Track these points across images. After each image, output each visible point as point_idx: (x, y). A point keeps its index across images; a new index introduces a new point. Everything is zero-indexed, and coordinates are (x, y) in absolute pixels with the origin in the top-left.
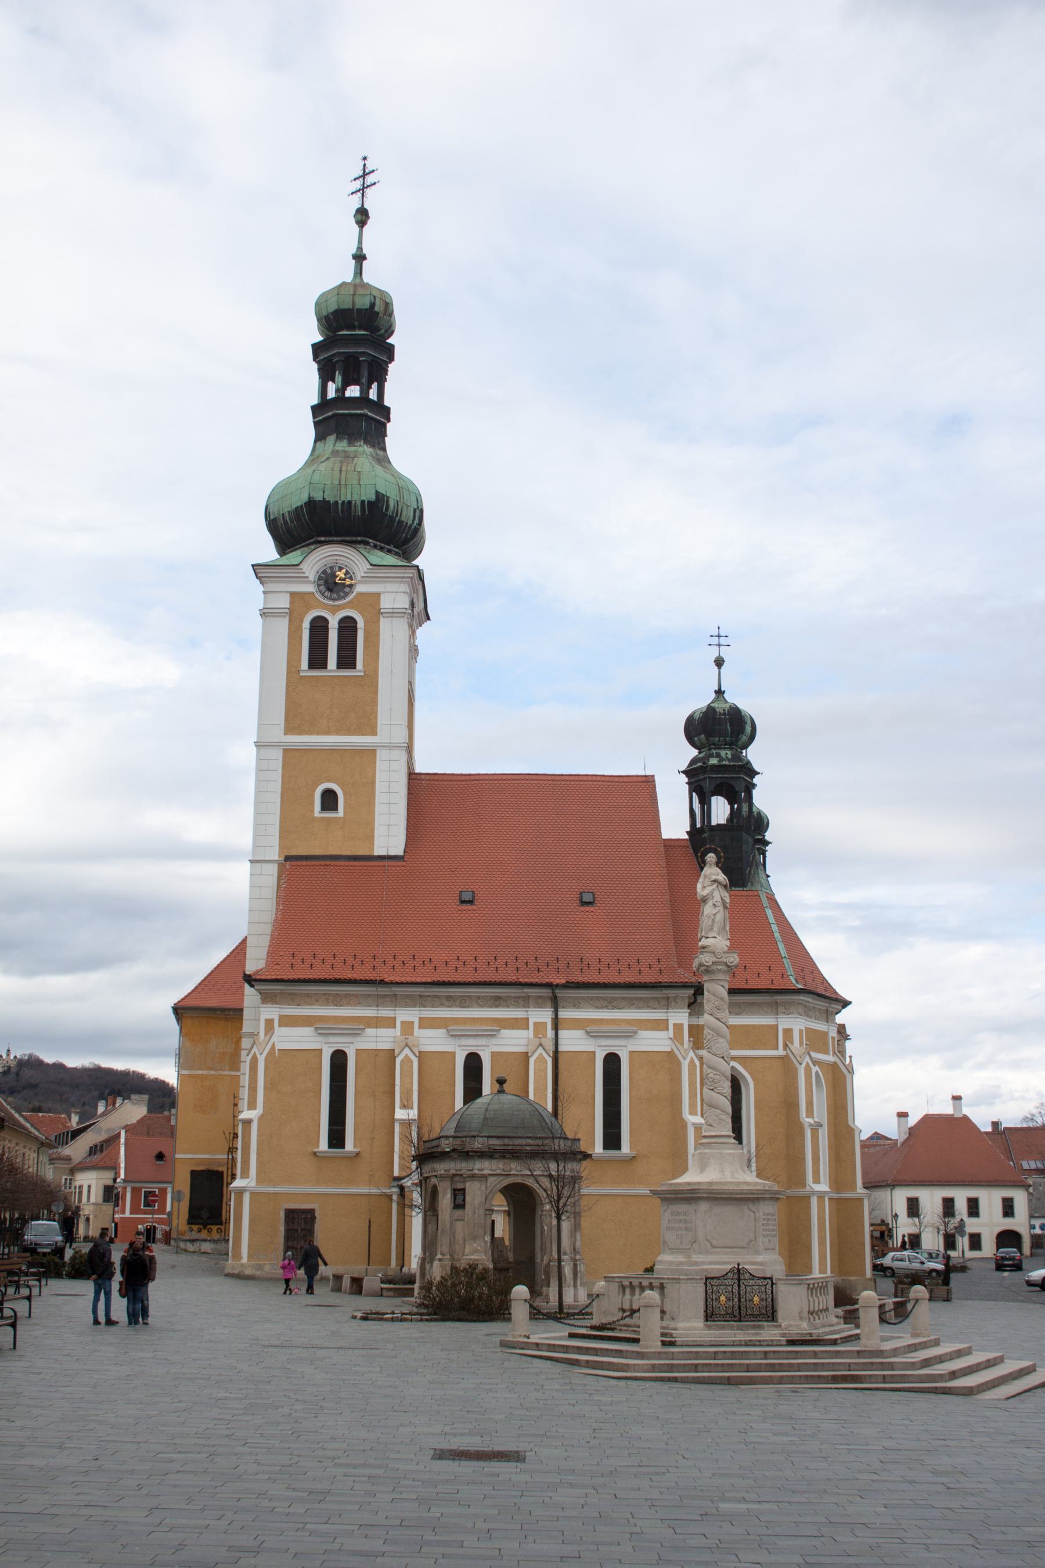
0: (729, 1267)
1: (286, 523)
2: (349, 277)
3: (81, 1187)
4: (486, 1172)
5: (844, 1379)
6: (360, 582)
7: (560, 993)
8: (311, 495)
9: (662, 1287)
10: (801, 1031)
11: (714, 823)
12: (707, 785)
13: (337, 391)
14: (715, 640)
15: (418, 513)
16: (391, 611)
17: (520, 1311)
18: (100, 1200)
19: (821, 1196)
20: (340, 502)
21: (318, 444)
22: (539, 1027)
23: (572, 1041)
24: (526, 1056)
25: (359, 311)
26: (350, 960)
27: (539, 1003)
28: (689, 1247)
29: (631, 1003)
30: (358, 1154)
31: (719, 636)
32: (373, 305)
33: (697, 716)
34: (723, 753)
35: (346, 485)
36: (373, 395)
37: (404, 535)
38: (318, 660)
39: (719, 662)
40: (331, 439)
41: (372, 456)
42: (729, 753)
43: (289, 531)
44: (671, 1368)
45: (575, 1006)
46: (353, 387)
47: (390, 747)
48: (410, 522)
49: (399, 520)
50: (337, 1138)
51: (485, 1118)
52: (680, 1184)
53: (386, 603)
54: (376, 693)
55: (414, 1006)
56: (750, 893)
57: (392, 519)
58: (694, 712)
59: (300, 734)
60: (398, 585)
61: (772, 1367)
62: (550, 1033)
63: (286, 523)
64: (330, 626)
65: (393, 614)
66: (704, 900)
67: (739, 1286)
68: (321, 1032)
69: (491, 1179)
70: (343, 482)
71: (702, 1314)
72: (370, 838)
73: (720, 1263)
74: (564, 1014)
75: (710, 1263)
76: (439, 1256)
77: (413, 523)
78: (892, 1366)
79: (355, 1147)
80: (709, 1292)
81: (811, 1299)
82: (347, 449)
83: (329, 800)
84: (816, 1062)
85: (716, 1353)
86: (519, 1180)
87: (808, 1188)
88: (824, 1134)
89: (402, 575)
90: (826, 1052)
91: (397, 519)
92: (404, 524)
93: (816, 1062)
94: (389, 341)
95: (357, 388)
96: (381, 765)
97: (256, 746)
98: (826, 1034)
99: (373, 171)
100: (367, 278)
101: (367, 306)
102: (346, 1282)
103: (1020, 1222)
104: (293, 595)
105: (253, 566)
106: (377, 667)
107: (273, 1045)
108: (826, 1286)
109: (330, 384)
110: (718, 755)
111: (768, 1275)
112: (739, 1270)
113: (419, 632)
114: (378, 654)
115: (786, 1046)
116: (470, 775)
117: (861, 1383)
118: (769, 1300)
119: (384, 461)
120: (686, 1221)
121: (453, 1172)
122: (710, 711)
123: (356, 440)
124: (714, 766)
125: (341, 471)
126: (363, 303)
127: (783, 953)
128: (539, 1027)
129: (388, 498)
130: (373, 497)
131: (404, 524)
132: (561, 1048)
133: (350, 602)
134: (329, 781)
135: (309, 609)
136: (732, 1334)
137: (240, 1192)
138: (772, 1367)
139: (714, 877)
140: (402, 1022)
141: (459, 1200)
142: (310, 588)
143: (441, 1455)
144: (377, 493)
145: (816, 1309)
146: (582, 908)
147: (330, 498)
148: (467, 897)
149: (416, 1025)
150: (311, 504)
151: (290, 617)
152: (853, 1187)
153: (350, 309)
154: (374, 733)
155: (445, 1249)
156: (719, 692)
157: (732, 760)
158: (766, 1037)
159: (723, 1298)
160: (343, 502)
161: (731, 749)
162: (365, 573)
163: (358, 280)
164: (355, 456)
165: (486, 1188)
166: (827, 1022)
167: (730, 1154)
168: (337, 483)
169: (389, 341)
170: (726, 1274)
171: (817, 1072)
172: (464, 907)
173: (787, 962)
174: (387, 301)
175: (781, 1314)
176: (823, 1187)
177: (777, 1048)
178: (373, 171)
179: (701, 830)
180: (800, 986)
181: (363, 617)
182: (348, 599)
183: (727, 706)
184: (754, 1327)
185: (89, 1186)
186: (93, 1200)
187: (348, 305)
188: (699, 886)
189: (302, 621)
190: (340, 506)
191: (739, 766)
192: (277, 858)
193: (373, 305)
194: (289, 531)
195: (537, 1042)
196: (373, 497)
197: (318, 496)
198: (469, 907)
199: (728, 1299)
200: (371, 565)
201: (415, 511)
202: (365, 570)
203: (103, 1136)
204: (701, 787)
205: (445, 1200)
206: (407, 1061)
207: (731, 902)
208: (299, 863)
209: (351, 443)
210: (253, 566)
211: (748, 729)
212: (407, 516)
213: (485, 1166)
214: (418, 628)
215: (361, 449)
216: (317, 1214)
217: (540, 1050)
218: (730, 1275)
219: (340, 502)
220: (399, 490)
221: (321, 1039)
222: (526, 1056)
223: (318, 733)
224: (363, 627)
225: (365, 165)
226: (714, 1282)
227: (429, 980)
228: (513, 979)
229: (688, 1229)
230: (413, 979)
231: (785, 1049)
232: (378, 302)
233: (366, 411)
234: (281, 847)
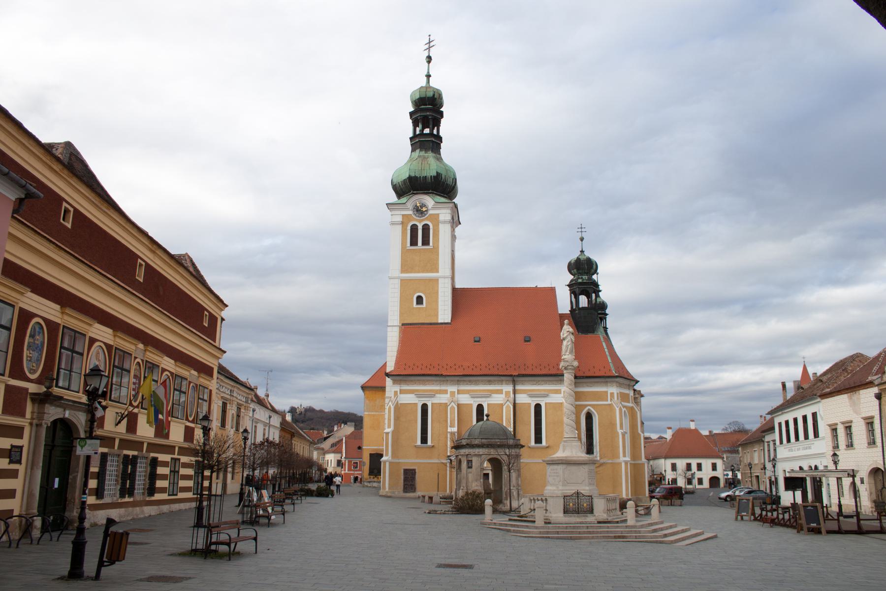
0: (574, 491)
1: (400, 186)
2: (424, 84)
3: (328, 460)
4: (481, 453)
5: (619, 537)
6: (431, 209)
7: (516, 379)
9: (546, 500)
10: (618, 393)
11: (581, 306)
12: (577, 291)
13: (420, 131)
14: (580, 230)
17: (488, 510)
18: (336, 466)
19: (626, 463)
21: (413, 153)
22: (507, 393)
23: (522, 399)
25: (428, 98)
26: (429, 366)
28: (557, 483)
29: (546, 382)
30: (433, 446)
31: (581, 228)
32: (434, 95)
33: (573, 262)
34: (584, 277)
35: (424, 169)
36: (435, 132)
38: (414, 242)
39: (582, 239)
40: (418, 151)
41: (435, 157)
42: (586, 277)
43: (401, 189)
44: (548, 533)
45: (522, 384)
46: (426, 129)
47: (444, 277)
48: (451, 184)
50: (424, 440)
51: (480, 431)
52: (554, 457)
53: (442, 218)
55: (455, 385)
56: (596, 336)
58: (572, 260)
60: (446, 210)
61: (590, 533)
62: (512, 395)
63: (400, 186)
64: (419, 228)
65: (445, 222)
66: (564, 339)
67: (578, 499)
68: (419, 396)
69: (483, 456)
70: (423, 168)
71: (562, 511)
72: (437, 315)
73: (570, 490)
74: (518, 387)
75: (566, 490)
76: (462, 488)
78: (640, 532)
79: (432, 443)
80: (566, 501)
81: (609, 505)
83: (420, 300)
84: (624, 407)
85: (566, 527)
86: (495, 456)
87: (621, 459)
88: (628, 437)
90: (629, 402)
93: (624, 407)
94: (441, 110)
95: (428, 129)
98: (628, 395)
100: (431, 84)
101: (432, 95)
102: (427, 498)
103: (719, 473)
104: (403, 215)
107: (398, 402)
108: (616, 499)
109: (417, 128)
110: (582, 278)
111: (590, 495)
112: (578, 493)
113: (457, 229)
115: (611, 400)
116: (478, 288)
117: (626, 539)
118: (591, 505)
119: (439, 159)
120: (557, 473)
121: (467, 453)
122: (578, 259)
123: (428, 150)
124: (580, 283)
125: (422, 164)
126: (430, 94)
127: (610, 361)
129: (442, 174)
130: (435, 174)
132: (517, 402)
133: (427, 218)
134: (419, 292)
135: (410, 221)
136: (574, 519)
137: (385, 462)
138: (590, 533)
139: (568, 330)
141: (470, 465)
143: (440, 566)
145: (611, 509)
146: (525, 343)
148: (477, 339)
149: (456, 393)
150: (410, 178)
152: (641, 459)
153: (424, 98)
154: (437, 271)
155: (464, 485)
156: (582, 252)
157: (588, 280)
158: (602, 396)
159: (571, 504)
161: (587, 275)
163: (428, 85)
164: (428, 158)
165: (481, 460)
166: (629, 389)
167: (575, 445)
169: (441, 110)
170: (573, 494)
171: (625, 411)
172: (476, 343)
173: (611, 365)
175: (595, 511)
176: (628, 459)
177: (607, 401)
179: (575, 310)
180: (617, 375)
181: (432, 223)
182: (426, 217)
183: (585, 257)
184: (584, 516)
185: (331, 460)
186: (333, 465)
187: (423, 96)
188: (562, 333)
191: (591, 283)
192: (398, 324)
194: (401, 189)
195: (507, 399)
196: (435, 174)
197: (413, 175)
198: (478, 343)
199: (573, 505)
201: (453, 179)
203: (337, 440)
204: (575, 292)
205: (464, 465)
207: (575, 341)
208: (408, 326)
209: (426, 152)
211: (594, 267)
212: (450, 181)
213: (481, 451)
216: (417, 471)
218: (574, 495)
221: (417, 399)
222: (501, 405)
223: (415, 272)
226: (567, 498)
227: (461, 374)
228: (496, 373)
229: (557, 476)
230: (455, 374)
231: (611, 401)
234: (400, 320)
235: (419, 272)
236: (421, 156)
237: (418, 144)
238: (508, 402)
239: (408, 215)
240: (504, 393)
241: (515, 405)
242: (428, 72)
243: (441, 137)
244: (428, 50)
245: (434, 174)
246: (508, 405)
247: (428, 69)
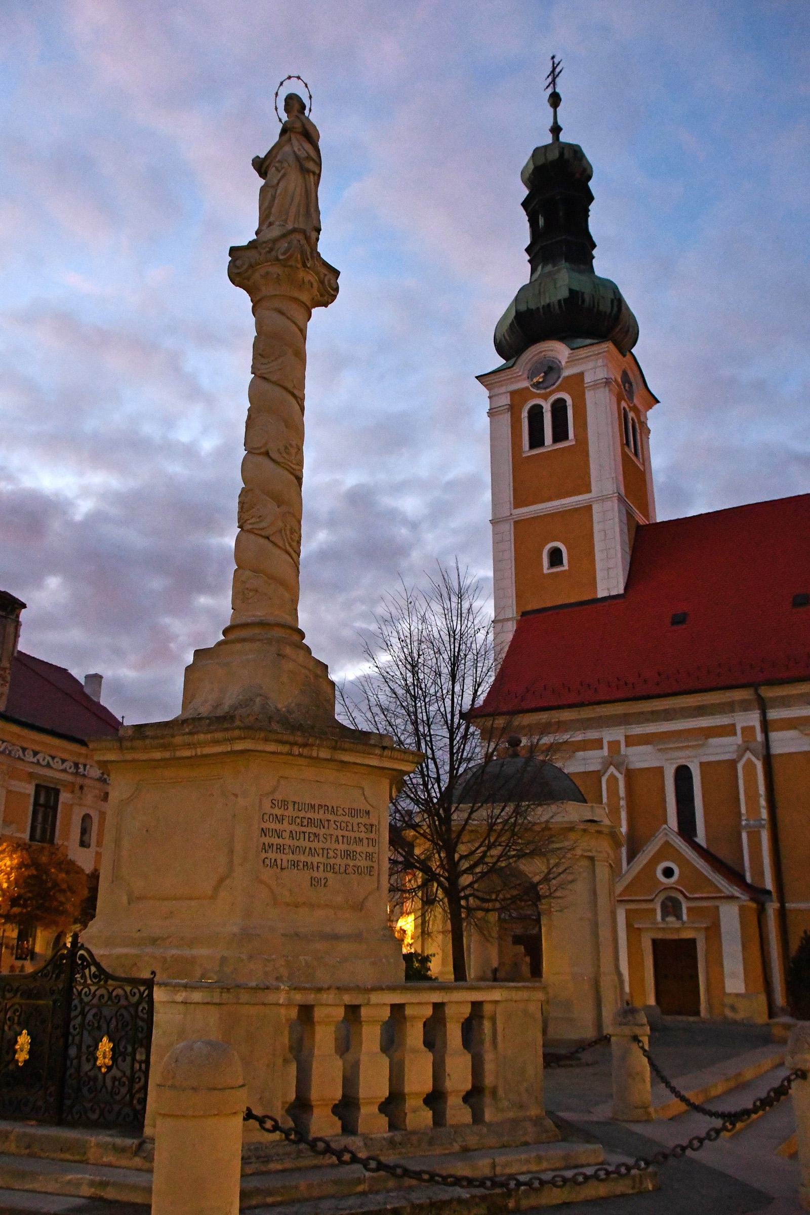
1: (506, 340)
6: (567, 367)
20: (541, 307)
22: (748, 731)
24: (733, 764)
27: (745, 706)
38: (536, 440)
47: (603, 499)
48: (609, 311)
53: (588, 379)
62: (760, 737)
63: (506, 340)
65: (595, 386)
70: (542, 290)
74: (773, 714)
77: (612, 310)
82: (552, 269)
83: (556, 557)
91: (595, 310)
96: (596, 517)
97: (492, 523)
104: (513, 394)
105: (477, 377)
128: (748, 731)
129: (583, 293)
133: (560, 385)
140: (609, 742)
142: (525, 384)
147: (532, 306)
154: (589, 491)
160: (543, 306)
162: (568, 358)
190: (541, 310)
197: (523, 308)
201: (612, 301)
206: (613, 778)
210: (477, 377)
212: (605, 307)
217: (748, 755)
222: (733, 764)
235: (550, 499)
238: (748, 755)
240: (739, 732)
241: (768, 760)
245: (564, 293)
246: (749, 760)
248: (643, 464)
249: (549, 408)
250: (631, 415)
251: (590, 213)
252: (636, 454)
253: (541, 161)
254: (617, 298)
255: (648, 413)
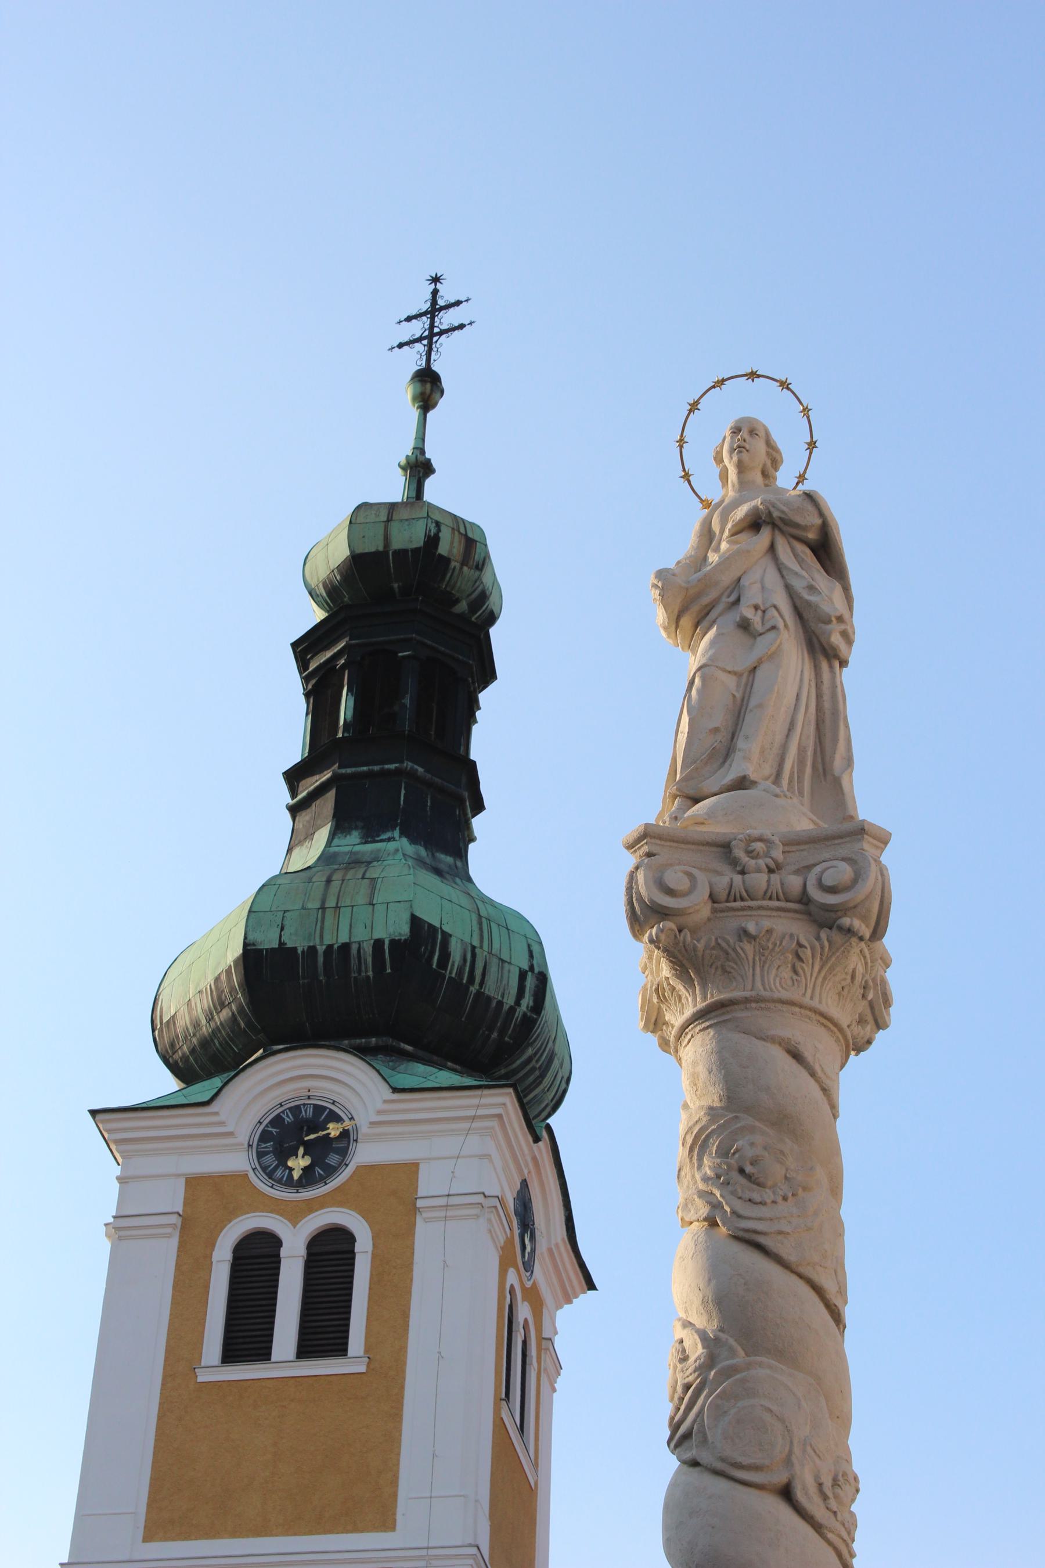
8: (250, 937)
15: (530, 982)
16: (442, 1201)
20: (321, 949)
25: (401, 554)
32: (432, 541)
35: (337, 907)
37: (495, 1035)
48: (509, 1001)
49: (479, 994)
54: (396, 1415)
57: (459, 988)
59: (188, 1538)
64: (284, 1252)
70: (331, 903)
77: (518, 1002)
82: (357, 848)
89: (471, 1113)
91: (474, 989)
92: (494, 1004)
99: (458, 303)
104: (194, 1183)
105: (94, 1113)
106: (403, 1349)
114: (405, 1315)
123: (387, 824)
125: (329, 881)
129: (446, 936)
130: (404, 930)
131: (494, 1004)
135: (232, 1213)
144: (416, 922)
147: (297, 941)
151: (181, 1237)
153: (376, 553)
154: (386, 1521)
160: (330, 947)
162: (379, 1112)
168: (318, 905)
174: (470, 535)
178: (458, 303)
189: (211, 1244)
190: (321, 959)
193: (432, 541)
197: (269, 940)
200: (395, 1090)
201: (523, 975)
202: (380, 1106)
210: (94, 1113)
214: (559, 1307)
215: (391, 846)
219: (321, 949)
220: (480, 924)
224: (369, 1248)
225: (435, 293)
232: (445, 535)
233: (408, 765)
236: (335, 855)
237: (331, 795)
239: (224, 1177)
242: (420, 450)
243: (475, 762)
244: (420, 347)
247: (421, 437)
248: (536, 1465)
249: (302, 1251)
250: (524, 1312)
251: (478, 714)
252: (522, 1428)
253: (373, 544)
254: (536, 970)
255: (559, 1313)
